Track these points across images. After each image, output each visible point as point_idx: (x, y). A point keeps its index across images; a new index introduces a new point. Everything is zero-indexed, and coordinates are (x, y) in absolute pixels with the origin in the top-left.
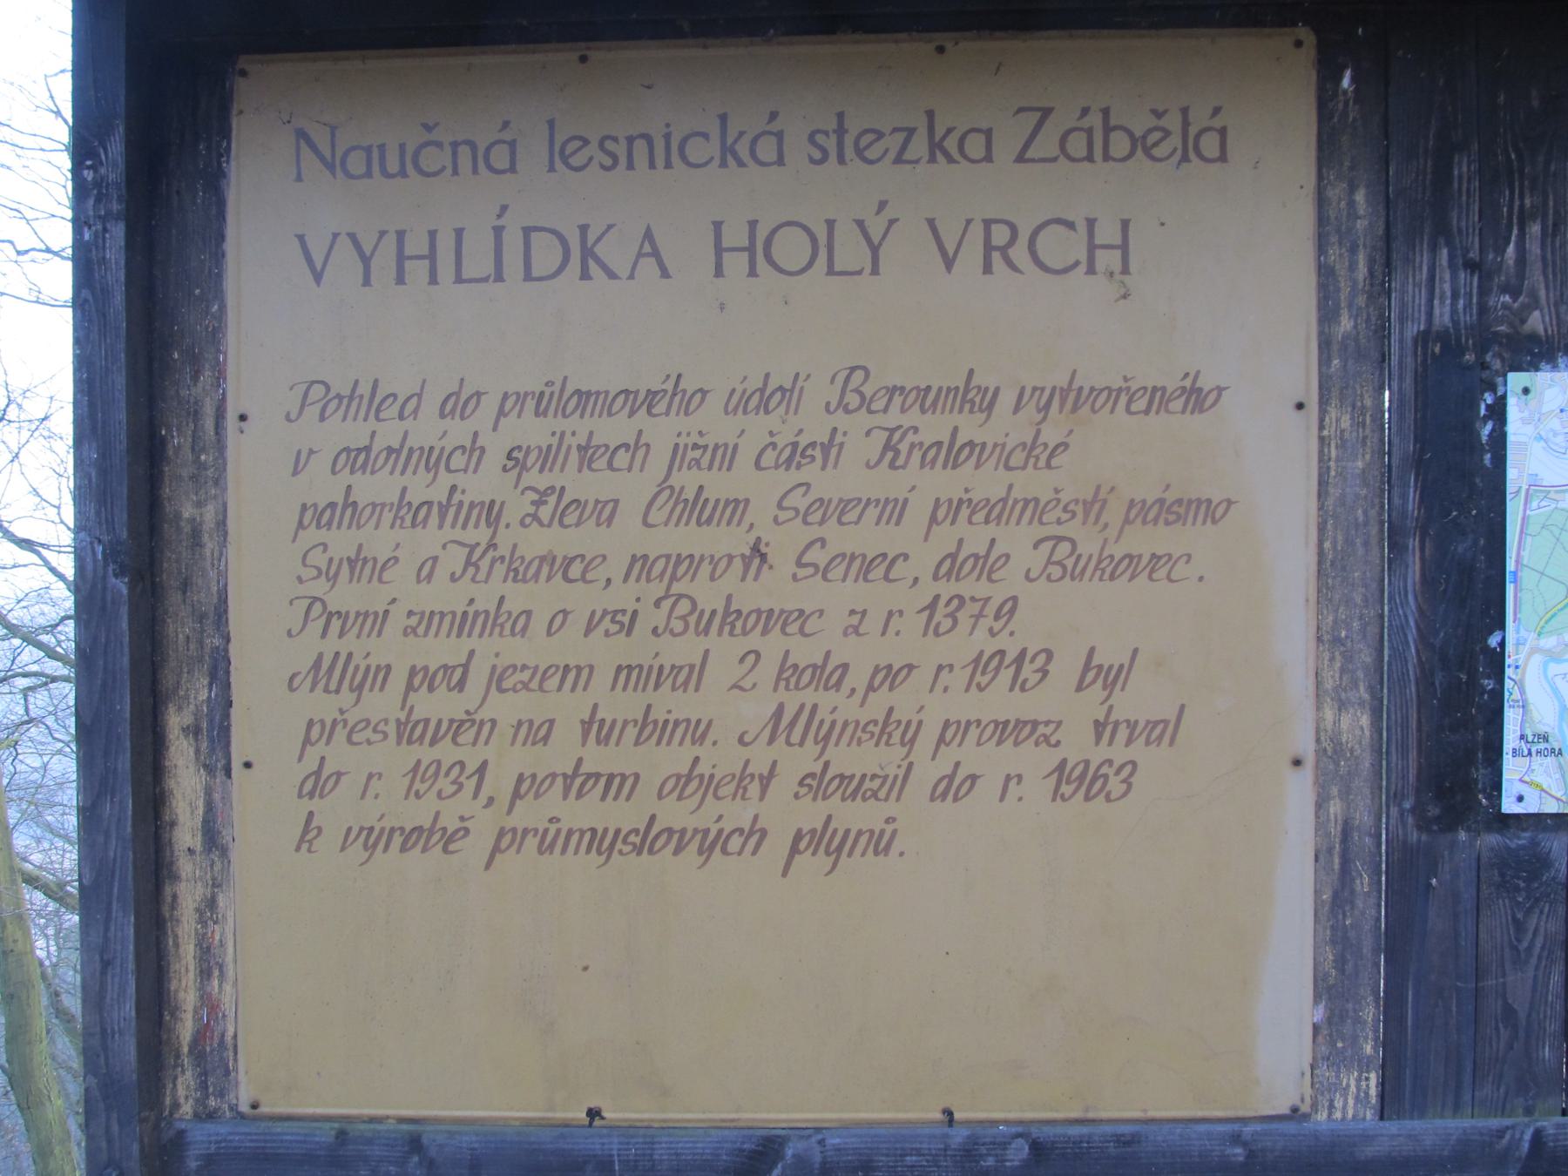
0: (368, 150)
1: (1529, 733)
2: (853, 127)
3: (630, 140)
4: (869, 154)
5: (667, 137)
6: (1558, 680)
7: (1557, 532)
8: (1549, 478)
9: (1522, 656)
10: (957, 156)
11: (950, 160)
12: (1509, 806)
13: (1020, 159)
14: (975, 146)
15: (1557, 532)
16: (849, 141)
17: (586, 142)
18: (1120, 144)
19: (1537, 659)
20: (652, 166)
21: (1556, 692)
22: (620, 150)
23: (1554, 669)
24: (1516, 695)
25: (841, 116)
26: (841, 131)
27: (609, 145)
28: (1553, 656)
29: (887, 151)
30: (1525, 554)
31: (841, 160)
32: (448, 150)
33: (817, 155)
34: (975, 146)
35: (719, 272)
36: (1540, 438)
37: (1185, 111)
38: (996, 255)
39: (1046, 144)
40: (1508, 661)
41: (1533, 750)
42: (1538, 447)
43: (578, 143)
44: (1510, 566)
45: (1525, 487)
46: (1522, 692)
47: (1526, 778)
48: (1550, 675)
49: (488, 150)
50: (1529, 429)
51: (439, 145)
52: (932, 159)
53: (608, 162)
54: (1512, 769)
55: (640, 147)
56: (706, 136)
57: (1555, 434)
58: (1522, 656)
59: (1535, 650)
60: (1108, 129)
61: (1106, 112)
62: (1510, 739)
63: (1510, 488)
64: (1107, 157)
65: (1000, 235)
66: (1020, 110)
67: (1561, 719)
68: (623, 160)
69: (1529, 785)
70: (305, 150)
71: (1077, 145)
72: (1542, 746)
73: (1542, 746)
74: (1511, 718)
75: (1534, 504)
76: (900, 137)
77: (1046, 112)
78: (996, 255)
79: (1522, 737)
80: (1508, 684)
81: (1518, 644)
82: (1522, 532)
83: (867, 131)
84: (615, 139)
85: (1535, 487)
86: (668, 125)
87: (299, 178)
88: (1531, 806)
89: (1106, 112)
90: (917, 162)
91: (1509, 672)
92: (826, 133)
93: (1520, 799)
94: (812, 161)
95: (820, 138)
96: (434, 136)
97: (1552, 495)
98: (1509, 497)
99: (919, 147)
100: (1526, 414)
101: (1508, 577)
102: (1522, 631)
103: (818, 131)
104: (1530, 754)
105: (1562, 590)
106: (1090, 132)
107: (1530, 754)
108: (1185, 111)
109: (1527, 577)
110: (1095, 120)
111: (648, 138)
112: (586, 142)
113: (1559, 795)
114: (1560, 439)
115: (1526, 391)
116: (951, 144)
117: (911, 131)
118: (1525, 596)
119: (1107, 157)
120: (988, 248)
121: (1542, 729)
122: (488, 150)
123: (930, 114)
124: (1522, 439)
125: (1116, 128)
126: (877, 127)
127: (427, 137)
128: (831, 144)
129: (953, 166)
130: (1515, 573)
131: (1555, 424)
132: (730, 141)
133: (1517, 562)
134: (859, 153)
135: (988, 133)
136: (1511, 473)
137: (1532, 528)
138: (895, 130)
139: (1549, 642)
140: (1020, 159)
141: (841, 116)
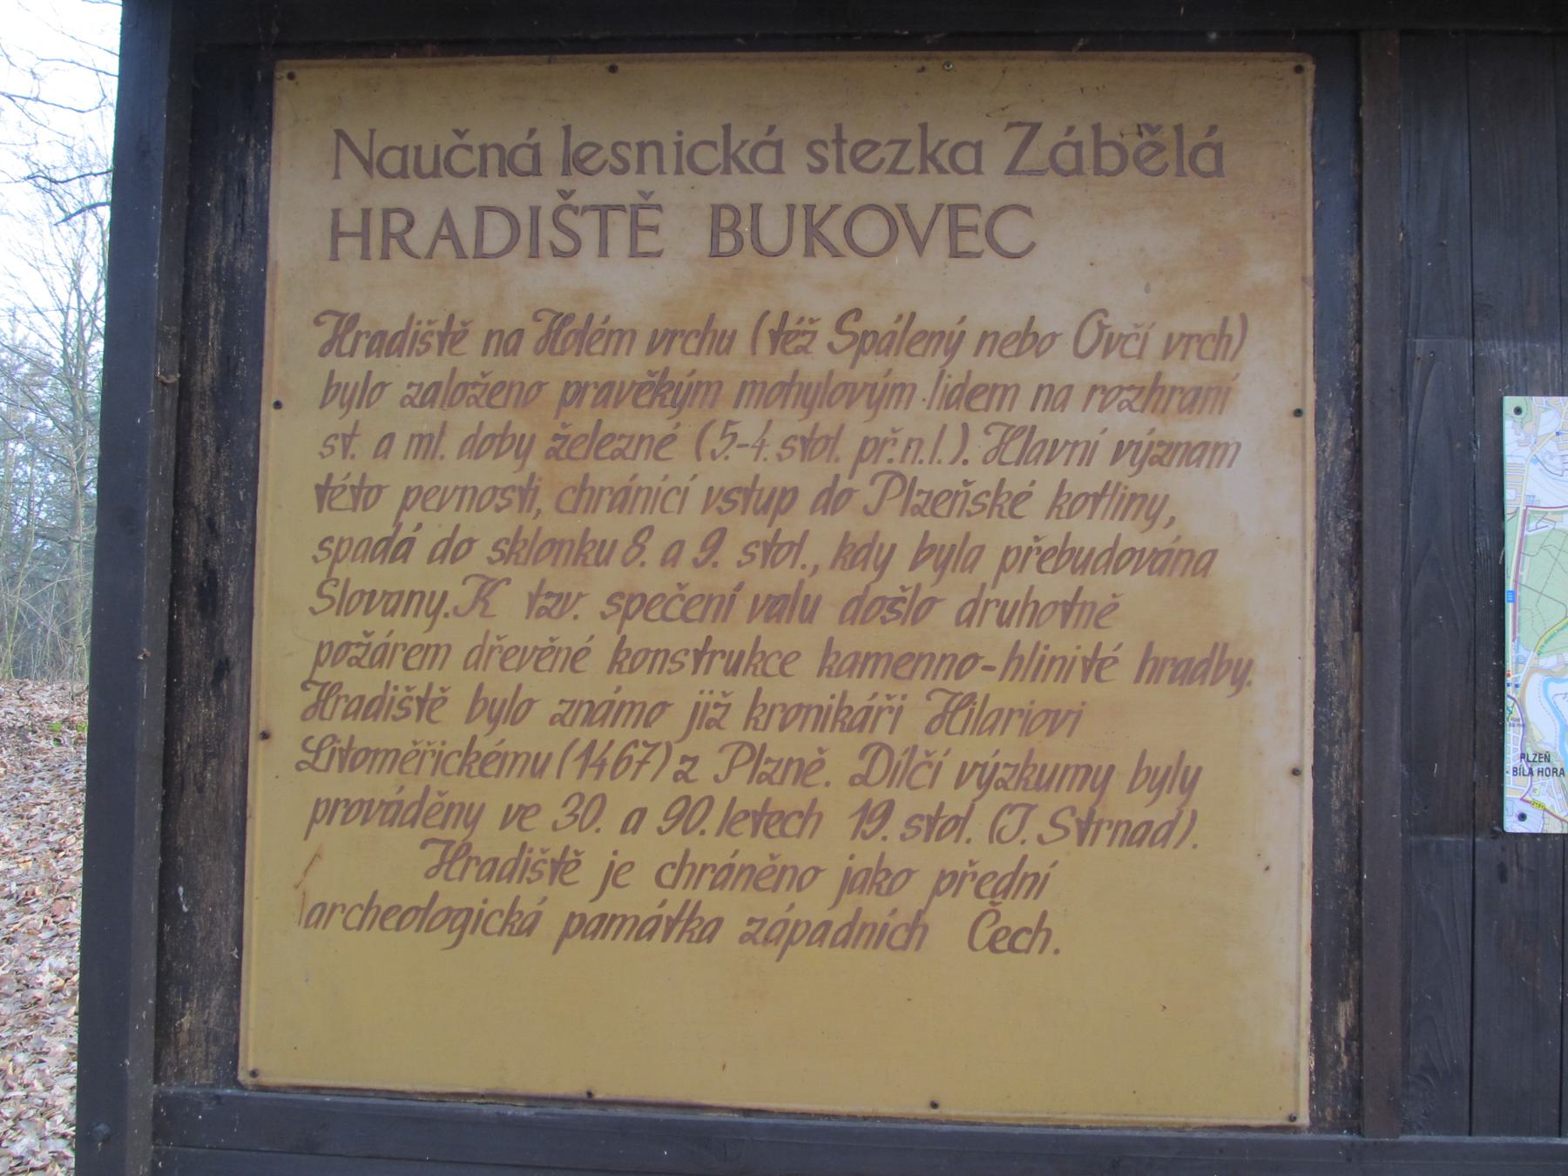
0: (404, 150)
1: (1530, 752)
2: (852, 136)
3: (642, 146)
4: (865, 163)
5: (679, 144)
6: (1559, 700)
7: (1555, 553)
8: (1546, 499)
9: (1522, 675)
10: (749, 166)
11: (941, 170)
12: (1511, 825)
13: (1011, 170)
14: (966, 159)
15: (1555, 553)
16: (847, 149)
17: (599, 148)
18: (1110, 158)
19: (1537, 679)
20: (661, 171)
21: (1556, 710)
22: (631, 155)
23: (1554, 688)
24: (1516, 713)
25: (839, 128)
26: (839, 141)
27: (622, 150)
28: (1552, 676)
29: (882, 161)
30: (1524, 574)
31: (840, 170)
32: (477, 152)
33: (816, 164)
34: (966, 159)
35: (335, 256)
36: (1536, 460)
37: (1179, 129)
38: (394, 243)
39: (1035, 155)
40: (1509, 680)
41: (1535, 769)
42: (1534, 469)
43: (592, 149)
44: (1510, 586)
45: (1522, 508)
46: (1522, 710)
47: (1528, 798)
48: (1551, 694)
49: (450, 152)
50: (1526, 452)
51: (469, 148)
52: (924, 170)
53: (619, 166)
54: (1513, 788)
55: (651, 152)
56: (714, 144)
57: (1552, 458)
58: (1522, 675)
59: (1536, 669)
60: (1098, 145)
61: (1097, 128)
62: (1511, 759)
63: (1509, 509)
64: (1098, 170)
65: (398, 223)
66: (1010, 125)
67: (1562, 738)
68: (634, 166)
69: (1534, 805)
70: (346, 154)
71: (1066, 155)
72: (1544, 765)
73: (1544, 765)
74: (1512, 737)
75: (1532, 525)
76: (897, 147)
77: (1036, 127)
78: (394, 243)
79: (1523, 756)
80: (1509, 702)
81: (1517, 663)
82: (1520, 552)
83: (865, 142)
84: (628, 145)
85: (1532, 508)
86: (680, 133)
87: (337, 176)
88: (1531, 826)
89: (1097, 128)
90: (909, 172)
91: (1509, 691)
92: (824, 143)
93: (1522, 817)
94: (812, 170)
95: (818, 149)
96: (466, 140)
97: (1549, 516)
98: (1507, 517)
99: (911, 159)
100: (1522, 436)
101: (1508, 597)
102: (1521, 649)
103: (814, 142)
104: (1531, 773)
105: (1562, 611)
106: (1078, 146)
107: (1531, 773)
108: (1179, 129)
109: (1523, 594)
110: (1084, 134)
111: (658, 145)
112: (599, 148)
113: (1562, 816)
114: (1557, 462)
115: (1518, 411)
116: (943, 157)
117: (905, 143)
118: (1524, 616)
119: (1098, 170)
120: (387, 235)
121: (1543, 748)
122: (450, 152)
123: (924, 127)
124: (1520, 461)
125: (1108, 143)
126: (872, 137)
127: (457, 141)
128: (830, 154)
129: (943, 176)
130: (1514, 593)
131: (1551, 446)
132: (733, 149)
133: (1516, 582)
134: (856, 163)
135: (978, 146)
136: (1509, 494)
137: (1530, 548)
138: (891, 142)
139: (1549, 661)
140: (1011, 170)
141: (839, 128)
